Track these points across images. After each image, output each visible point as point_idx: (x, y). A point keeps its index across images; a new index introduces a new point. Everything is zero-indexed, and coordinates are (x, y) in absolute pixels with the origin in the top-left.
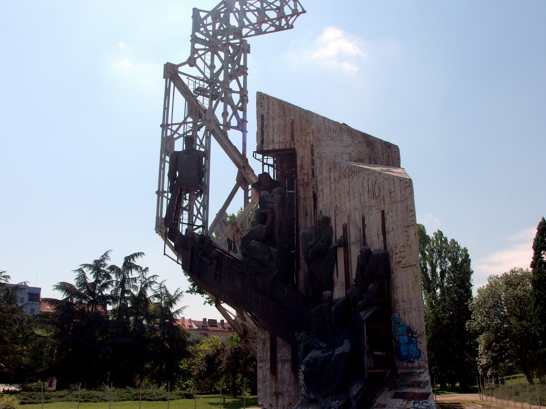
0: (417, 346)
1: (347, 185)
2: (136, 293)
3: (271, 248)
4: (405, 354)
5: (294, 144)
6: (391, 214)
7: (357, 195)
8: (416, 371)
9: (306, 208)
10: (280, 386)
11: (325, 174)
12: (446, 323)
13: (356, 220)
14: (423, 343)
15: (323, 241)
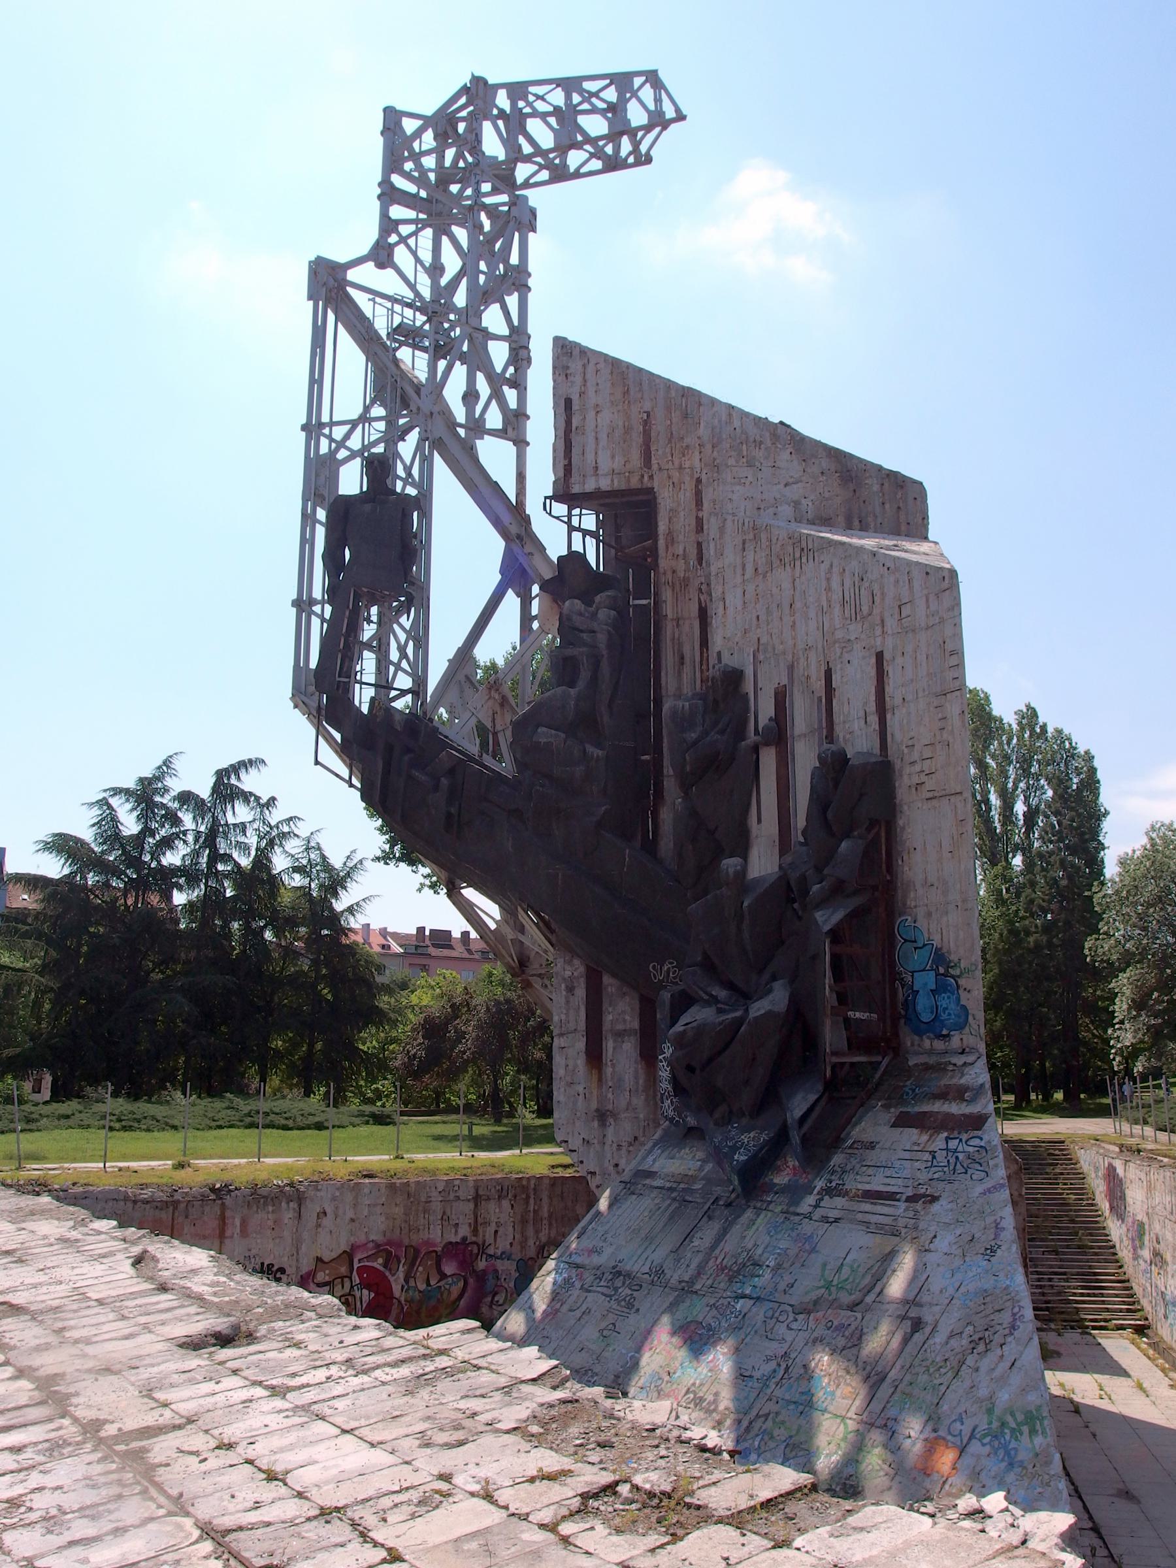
0: (958, 999)
1: (786, 585)
2: (245, 862)
3: (590, 749)
4: (926, 1017)
5: (651, 477)
6: (899, 660)
7: (812, 614)
8: (954, 1060)
9: (680, 645)
10: (610, 1095)
11: (731, 556)
12: (1036, 941)
13: (808, 677)
14: (974, 992)
15: (722, 732)
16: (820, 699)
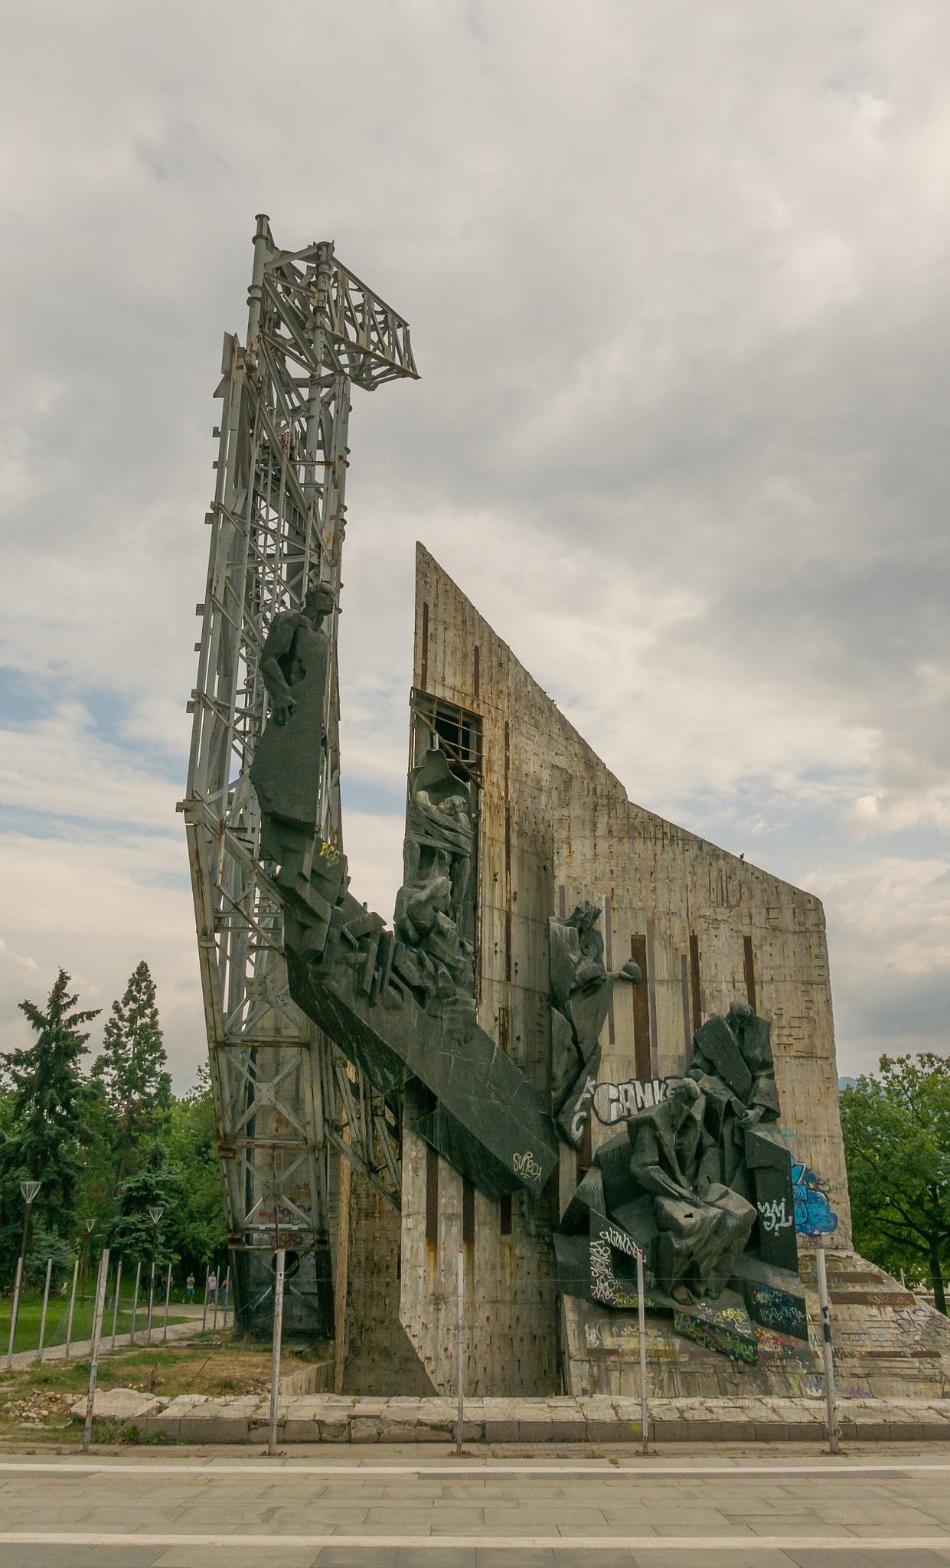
6: (767, 948)
16: (684, 957)
